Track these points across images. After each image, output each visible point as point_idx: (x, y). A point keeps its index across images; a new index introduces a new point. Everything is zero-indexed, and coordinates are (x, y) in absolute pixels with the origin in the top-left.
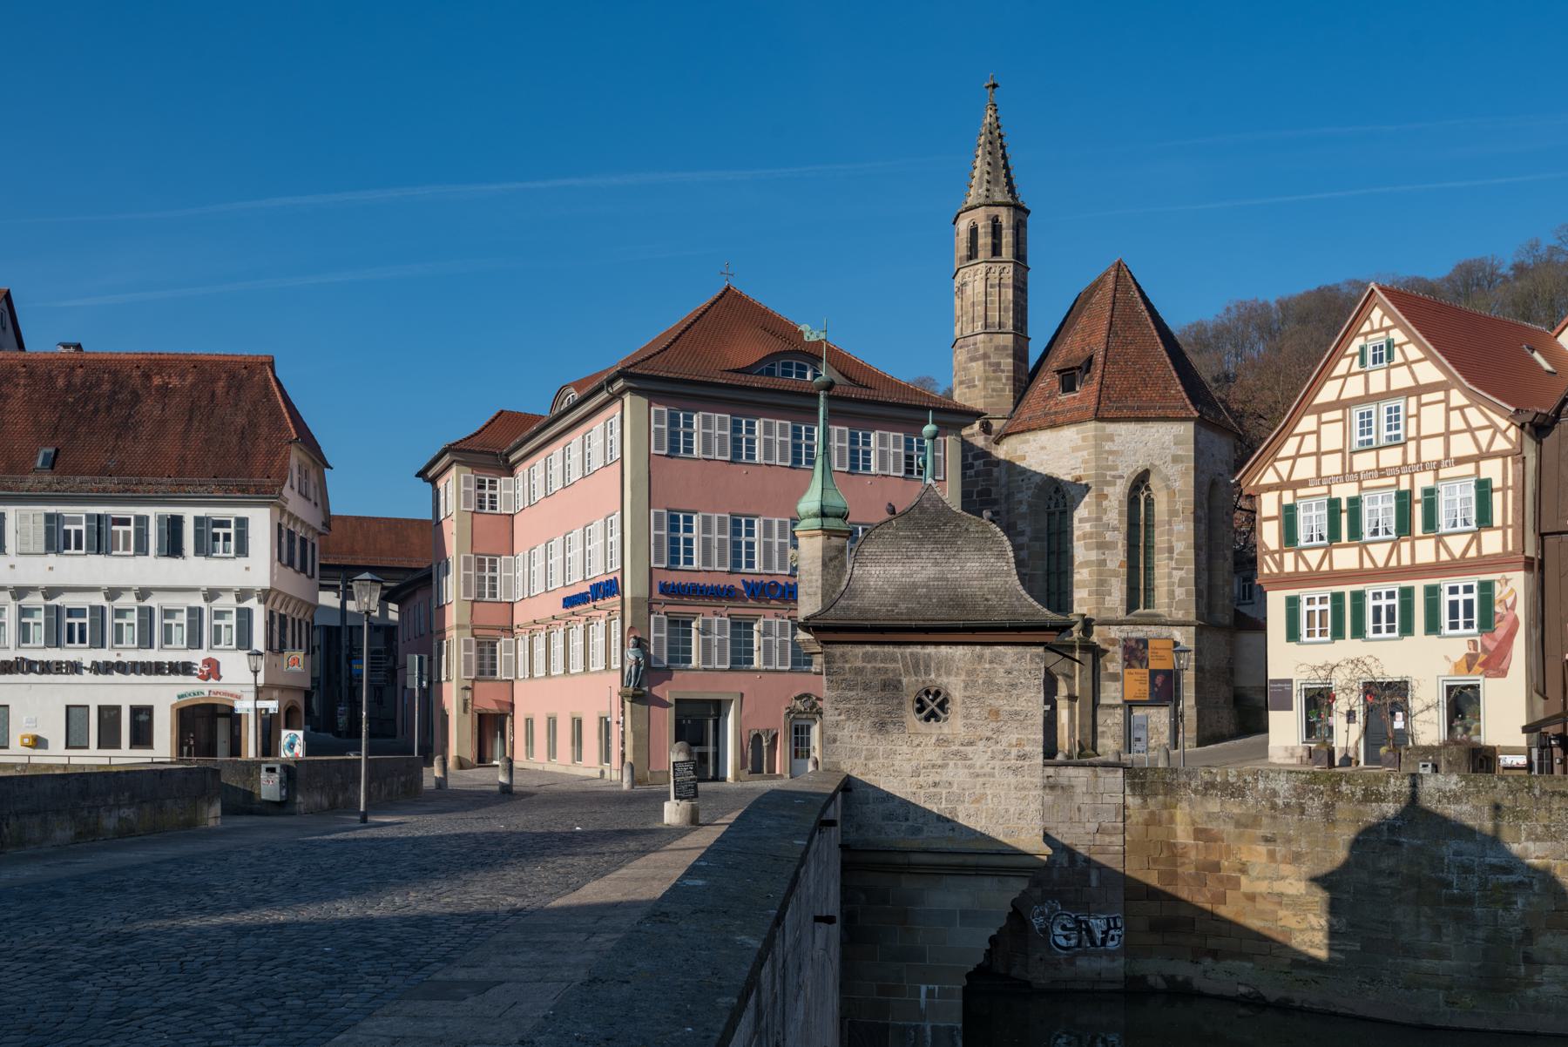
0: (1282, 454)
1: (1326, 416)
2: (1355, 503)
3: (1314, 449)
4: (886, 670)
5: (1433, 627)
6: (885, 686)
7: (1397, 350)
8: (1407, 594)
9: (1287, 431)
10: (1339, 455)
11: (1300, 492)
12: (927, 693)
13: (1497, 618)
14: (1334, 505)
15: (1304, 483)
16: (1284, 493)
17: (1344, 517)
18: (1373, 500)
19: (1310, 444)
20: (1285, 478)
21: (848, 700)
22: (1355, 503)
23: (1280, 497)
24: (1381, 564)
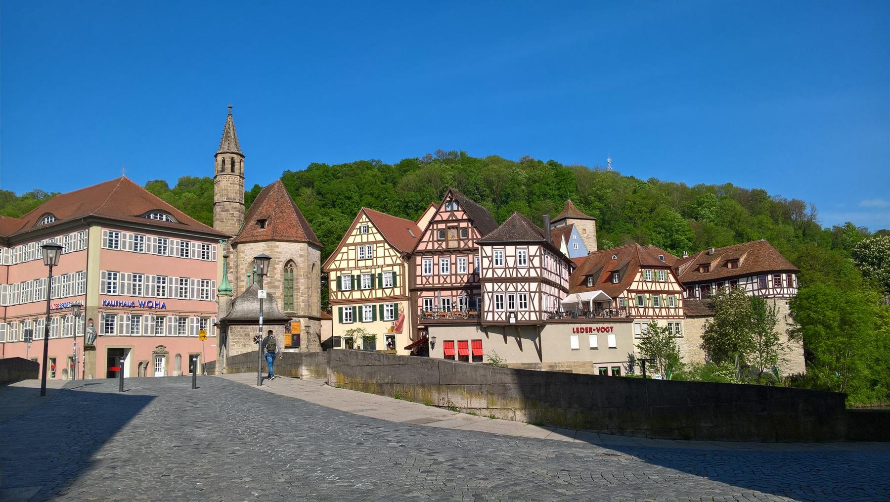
0: (336, 259)
1: (350, 248)
2: (359, 276)
3: (347, 258)
4: (246, 331)
5: (382, 318)
6: (245, 335)
8: (374, 307)
9: (338, 252)
10: (354, 261)
11: (343, 272)
12: (256, 337)
13: (399, 315)
14: (353, 276)
15: (344, 269)
16: (338, 272)
17: (356, 281)
19: (345, 256)
21: (236, 339)
22: (359, 276)
23: (336, 273)
24: (367, 297)
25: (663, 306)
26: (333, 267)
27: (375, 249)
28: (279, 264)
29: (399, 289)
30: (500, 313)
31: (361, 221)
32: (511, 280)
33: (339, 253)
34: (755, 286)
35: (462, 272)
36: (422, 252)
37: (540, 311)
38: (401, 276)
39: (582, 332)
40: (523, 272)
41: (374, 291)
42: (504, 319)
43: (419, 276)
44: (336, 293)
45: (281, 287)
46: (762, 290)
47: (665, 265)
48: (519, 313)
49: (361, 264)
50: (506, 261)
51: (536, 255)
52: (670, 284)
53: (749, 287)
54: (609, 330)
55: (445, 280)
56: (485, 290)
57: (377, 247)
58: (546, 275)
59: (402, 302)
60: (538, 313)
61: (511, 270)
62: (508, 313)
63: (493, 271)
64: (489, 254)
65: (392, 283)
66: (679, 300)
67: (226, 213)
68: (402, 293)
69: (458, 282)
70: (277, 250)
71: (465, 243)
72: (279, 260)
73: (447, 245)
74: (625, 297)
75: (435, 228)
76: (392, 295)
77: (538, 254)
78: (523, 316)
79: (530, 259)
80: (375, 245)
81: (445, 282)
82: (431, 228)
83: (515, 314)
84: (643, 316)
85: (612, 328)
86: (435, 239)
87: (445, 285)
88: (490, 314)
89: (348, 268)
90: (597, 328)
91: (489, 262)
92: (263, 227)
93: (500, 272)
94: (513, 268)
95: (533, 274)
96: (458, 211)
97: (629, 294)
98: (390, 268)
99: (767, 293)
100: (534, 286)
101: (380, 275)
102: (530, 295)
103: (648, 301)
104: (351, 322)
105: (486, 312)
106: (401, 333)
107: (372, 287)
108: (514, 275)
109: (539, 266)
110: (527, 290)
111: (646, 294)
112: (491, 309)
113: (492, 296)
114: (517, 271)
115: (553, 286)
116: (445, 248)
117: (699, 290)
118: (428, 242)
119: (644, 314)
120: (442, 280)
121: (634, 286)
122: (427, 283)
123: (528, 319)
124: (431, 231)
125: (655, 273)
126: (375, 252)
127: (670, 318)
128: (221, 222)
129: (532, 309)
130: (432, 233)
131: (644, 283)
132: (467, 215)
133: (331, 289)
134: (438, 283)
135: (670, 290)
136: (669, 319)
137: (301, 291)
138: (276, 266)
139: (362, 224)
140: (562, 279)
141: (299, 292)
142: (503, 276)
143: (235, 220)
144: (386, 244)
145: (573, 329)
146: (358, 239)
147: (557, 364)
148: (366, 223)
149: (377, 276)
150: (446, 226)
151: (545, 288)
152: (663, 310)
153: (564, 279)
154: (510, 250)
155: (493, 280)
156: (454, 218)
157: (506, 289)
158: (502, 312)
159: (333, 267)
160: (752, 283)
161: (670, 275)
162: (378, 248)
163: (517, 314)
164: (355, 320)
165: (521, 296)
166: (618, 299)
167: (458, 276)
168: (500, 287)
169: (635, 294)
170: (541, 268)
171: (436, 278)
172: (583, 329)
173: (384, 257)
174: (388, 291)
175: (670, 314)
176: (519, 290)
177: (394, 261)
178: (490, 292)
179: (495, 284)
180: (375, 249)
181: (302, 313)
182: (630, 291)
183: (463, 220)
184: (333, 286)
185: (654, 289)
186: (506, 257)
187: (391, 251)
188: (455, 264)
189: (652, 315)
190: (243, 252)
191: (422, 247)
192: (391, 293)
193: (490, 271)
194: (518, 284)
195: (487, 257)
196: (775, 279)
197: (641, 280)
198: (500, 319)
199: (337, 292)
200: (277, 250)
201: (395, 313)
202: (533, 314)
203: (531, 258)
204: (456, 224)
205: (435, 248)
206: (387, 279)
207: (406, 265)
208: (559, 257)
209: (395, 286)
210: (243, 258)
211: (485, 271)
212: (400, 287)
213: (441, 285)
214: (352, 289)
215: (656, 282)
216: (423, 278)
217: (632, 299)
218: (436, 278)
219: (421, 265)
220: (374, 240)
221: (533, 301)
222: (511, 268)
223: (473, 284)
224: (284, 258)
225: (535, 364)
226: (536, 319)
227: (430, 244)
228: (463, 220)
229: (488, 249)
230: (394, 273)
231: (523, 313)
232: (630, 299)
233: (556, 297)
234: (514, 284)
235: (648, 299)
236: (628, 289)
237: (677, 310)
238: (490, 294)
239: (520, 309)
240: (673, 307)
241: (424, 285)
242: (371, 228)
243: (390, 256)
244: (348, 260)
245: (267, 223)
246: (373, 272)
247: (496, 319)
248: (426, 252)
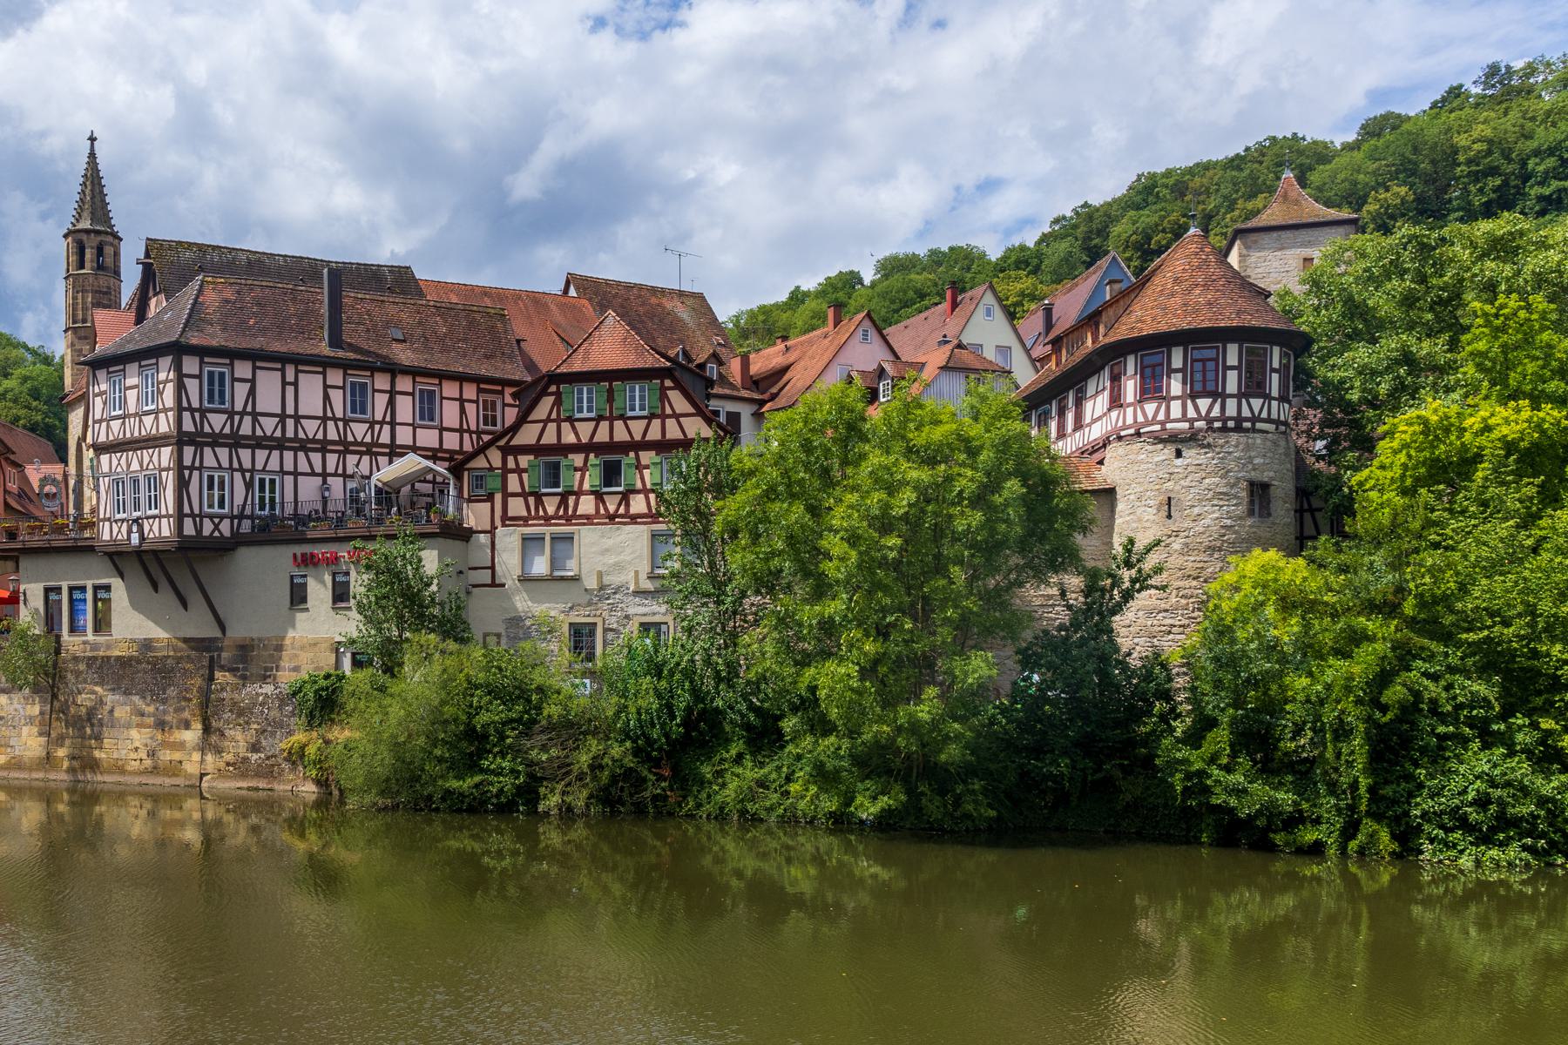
52: (670, 423)
63: (108, 426)
74: (491, 469)
84: (556, 517)
88: (107, 524)
95: (164, 428)
108: (136, 434)
119: (561, 513)
121: (528, 435)
125: (610, 392)
131: (566, 426)
135: (669, 436)
145: (295, 555)
147: (256, 642)
157: (129, 466)
158: (123, 521)
166: (466, 473)
169: (532, 457)
182: (507, 451)
185: (602, 436)
189: (592, 511)
197: (554, 416)
217: (519, 471)
231: (151, 521)
232: (512, 471)
236: (502, 443)
239: (149, 513)
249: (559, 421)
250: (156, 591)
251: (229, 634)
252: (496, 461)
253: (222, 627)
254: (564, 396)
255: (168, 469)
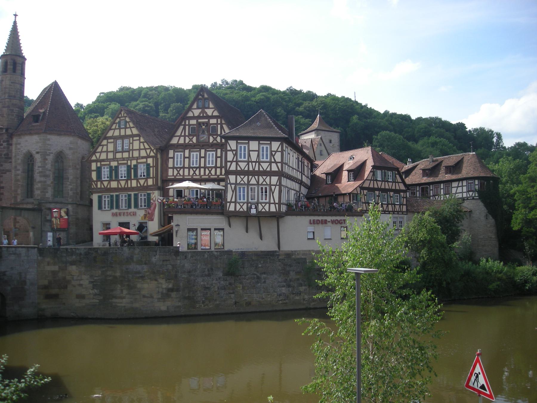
1: (109, 141)
7: (128, 124)
8: (130, 196)
11: (103, 163)
14: (111, 167)
17: (114, 172)
18: (104, 168)
19: (105, 149)
20: (98, 158)
24: (123, 186)
25: (390, 203)
26: (94, 158)
27: (131, 142)
28: (50, 155)
29: (151, 180)
30: (241, 204)
31: (120, 116)
32: (254, 173)
33: (100, 145)
34: (465, 189)
35: (211, 165)
36: (174, 146)
37: (280, 204)
38: (154, 168)
39: (317, 224)
40: (265, 166)
41: (129, 182)
42: (245, 210)
43: (171, 168)
44: (96, 182)
45: (51, 176)
46: (470, 193)
47: (392, 166)
48: (259, 205)
49: (119, 156)
50: (249, 155)
51: (278, 150)
52: (397, 184)
53: (460, 190)
54: (342, 222)
55: (194, 172)
56: (229, 182)
57: (133, 140)
58: (286, 170)
59: (154, 192)
60: (277, 205)
61: (254, 164)
62: (249, 205)
63: (237, 164)
64: (234, 148)
65: (145, 174)
66: (404, 198)
67: (6, 109)
68: (154, 184)
69: (207, 174)
70: (48, 142)
71: (214, 138)
72: (50, 152)
73: (197, 140)
75: (187, 123)
76: (145, 185)
77: (280, 149)
78: (263, 207)
79: (271, 154)
80: (131, 139)
81: (194, 175)
82: (183, 123)
83: (255, 205)
85: (344, 220)
86: (187, 134)
87: (194, 177)
88: (233, 205)
89: (107, 160)
90: (331, 220)
91: (233, 156)
92: (37, 121)
93: (243, 165)
94: (256, 162)
95: (274, 168)
96: (209, 108)
97: (362, 191)
98: (144, 160)
99: (473, 195)
100: (274, 179)
101: (136, 167)
102: (271, 189)
103: (377, 197)
104: (109, 209)
105: (229, 202)
106: (152, 220)
107: (129, 178)
108: (257, 169)
109: (280, 161)
110: (268, 183)
111: (376, 192)
112: (233, 200)
113: (235, 188)
114: (259, 164)
115: (294, 181)
116: (195, 142)
117: (419, 191)
118: (180, 136)
120: (192, 172)
122: (178, 175)
123: (267, 210)
124: (183, 126)
125: (385, 173)
126: (131, 145)
127: (395, 213)
128: (2, 117)
129: (272, 201)
130: (184, 129)
131: (375, 182)
132: (219, 112)
133: (92, 179)
134: (187, 175)
136: (394, 214)
137: (69, 181)
138: (47, 157)
139: (121, 118)
140: (304, 176)
141: (68, 181)
142: (246, 169)
143: (15, 116)
144: (141, 138)
145: (310, 220)
146: (117, 133)
148: (124, 118)
149: (132, 167)
150: (197, 121)
151: (284, 181)
152: (390, 206)
153: (305, 176)
154: (254, 145)
155: (236, 173)
156: (205, 115)
159: (94, 158)
160: (462, 186)
161: (397, 176)
162: (134, 142)
163: (258, 205)
164: (112, 208)
165: (262, 188)
167: (207, 170)
168: (242, 179)
169: (367, 191)
170: (282, 162)
171: (186, 171)
172: (319, 220)
173: (140, 150)
174: (142, 182)
175: (396, 210)
176: (260, 183)
177: (148, 153)
178: (233, 184)
179: (238, 177)
180: (131, 142)
181: (70, 200)
183: (213, 117)
184: (94, 175)
185: (383, 187)
186: (249, 151)
187: (145, 144)
188: (205, 157)
190: (20, 144)
191: (174, 141)
192: (144, 183)
193: (234, 164)
194: (260, 177)
195: (232, 150)
196: (481, 184)
197: (372, 179)
198: (241, 210)
199: (97, 181)
200: (48, 142)
201: (149, 203)
202: (273, 206)
203: (273, 153)
204: (207, 120)
205: (187, 142)
206: (141, 169)
207: (159, 156)
208: (302, 155)
209: (148, 177)
210: (19, 149)
211: (229, 164)
212: (153, 178)
213: (190, 177)
214: (110, 180)
215: (385, 181)
216: (175, 170)
218: (186, 171)
219: (173, 158)
220: (131, 134)
221: (273, 193)
222: (254, 162)
223: (220, 177)
224: (55, 149)
225: (273, 251)
226: (275, 211)
227: (182, 138)
228: (213, 117)
229: (232, 144)
230: (148, 166)
231: (263, 205)
233: (296, 191)
234: (256, 177)
235: (377, 196)
237: (401, 206)
238: (233, 186)
240: (398, 203)
241: (175, 176)
242: (128, 122)
243: (145, 149)
244: (107, 152)
245: (41, 118)
246: (129, 164)
247: (237, 210)
248: (177, 146)
249: (374, 180)
250: (247, 232)
251: (281, 249)
252: (359, 193)
253: (279, 248)
254: (375, 173)
255: (276, 185)
